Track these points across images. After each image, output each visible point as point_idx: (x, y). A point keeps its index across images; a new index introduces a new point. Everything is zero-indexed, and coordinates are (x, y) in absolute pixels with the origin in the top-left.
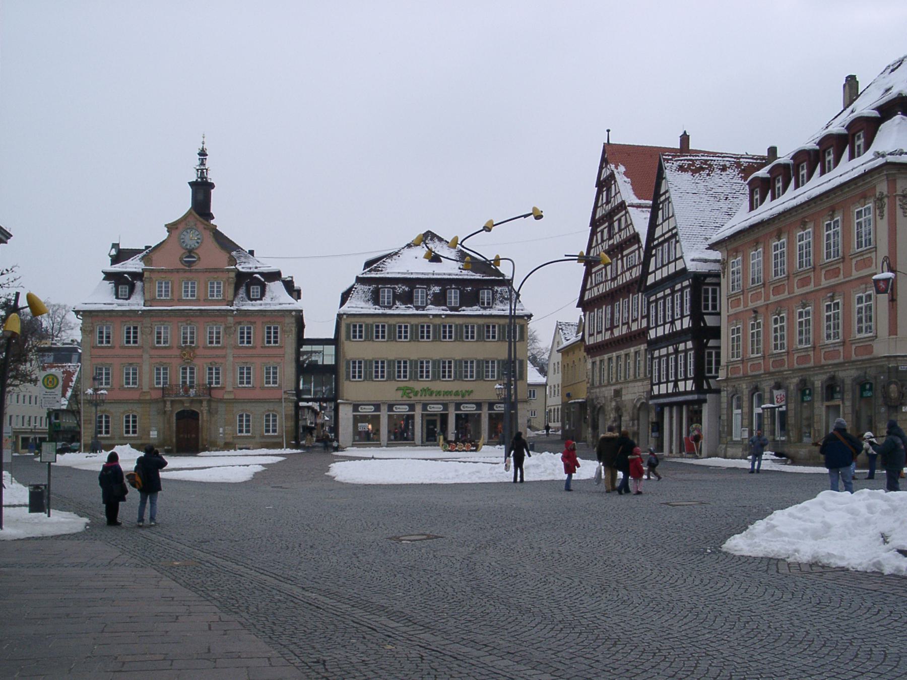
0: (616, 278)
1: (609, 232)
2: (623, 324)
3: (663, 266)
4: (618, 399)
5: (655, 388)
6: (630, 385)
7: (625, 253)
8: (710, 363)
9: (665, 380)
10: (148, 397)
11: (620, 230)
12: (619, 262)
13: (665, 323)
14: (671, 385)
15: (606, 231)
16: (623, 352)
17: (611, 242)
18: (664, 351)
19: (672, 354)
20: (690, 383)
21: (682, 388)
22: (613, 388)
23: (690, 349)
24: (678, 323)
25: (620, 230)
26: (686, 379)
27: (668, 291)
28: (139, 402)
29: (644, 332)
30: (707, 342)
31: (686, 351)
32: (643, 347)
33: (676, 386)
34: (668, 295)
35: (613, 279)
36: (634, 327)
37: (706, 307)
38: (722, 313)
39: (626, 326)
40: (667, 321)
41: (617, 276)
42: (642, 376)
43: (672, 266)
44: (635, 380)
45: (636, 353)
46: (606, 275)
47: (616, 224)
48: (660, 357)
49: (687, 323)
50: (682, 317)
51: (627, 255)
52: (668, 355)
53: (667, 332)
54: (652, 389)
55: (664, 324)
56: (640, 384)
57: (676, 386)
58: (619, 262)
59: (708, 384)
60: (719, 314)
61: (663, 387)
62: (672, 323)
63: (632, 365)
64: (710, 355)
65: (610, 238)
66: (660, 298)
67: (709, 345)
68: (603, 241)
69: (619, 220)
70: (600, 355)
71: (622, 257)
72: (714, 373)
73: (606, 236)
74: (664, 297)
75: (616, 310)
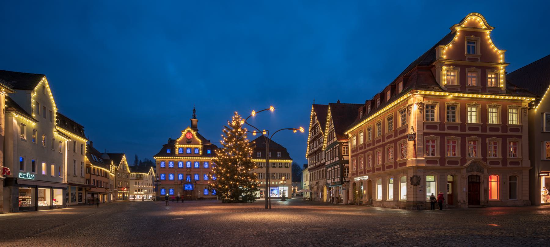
0: (316, 147)
1: (314, 132)
2: (319, 161)
3: (330, 141)
4: (318, 185)
5: (328, 181)
6: (321, 180)
7: (319, 139)
8: (345, 172)
9: (336, 177)
10: (177, 183)
11: (318, 132)
12: (317, 142)
13: (331, 159)
14: (333, 180)
15: (313, 132)
16: (319, 170)
17: (315, 136)
18: (330, 169)
19: (333, 170)
20: (338, 179)
21: (336, 181)
22: (316, 181)
23: (339, 168)
24: (335, 159)
25: (318, 132)
26: (337, 177)
27: (331, 149)
28: (174, 185)
29: (324, 164)
30: (344, 165)
31: (337, 168)
32: (324, 168)
33: (334, 180)
34: (332, 150)
35: (315, 148)
36: (322, 162)
37: (344, 154)
38: (349, 155)
39: (320, 162)
40: (331, 159)
41: (317, 146)
42: (324, 177)
43: (332, 140)
44: (322, 179)
45: (323, 170)
46: (314, 146)
47: (316, 130)
48: (329, 171)
49: (337, 159)
50: (336, 157)
51: (320, 139)
52: (332, 170)
53: (331, 162)
54: (327, 181)
55: (330, 160)
56: (324, 180)
57: (334, 180)
58: (317, 142)
59: (345, 179)
60: (348, 156)
61: (330, 180)
62: (333, 159)
63: (321, 174)
64: (345, 169)
65: (315, 135)
66: (329, 152)
67: (345, 166)
68: (313, 136)
69: (317, 128)
70: (312, 172)
71: (318, 140)
72: (347, 176)
73: (313, 134)
74: (330, 151)
75: (317, 157)
